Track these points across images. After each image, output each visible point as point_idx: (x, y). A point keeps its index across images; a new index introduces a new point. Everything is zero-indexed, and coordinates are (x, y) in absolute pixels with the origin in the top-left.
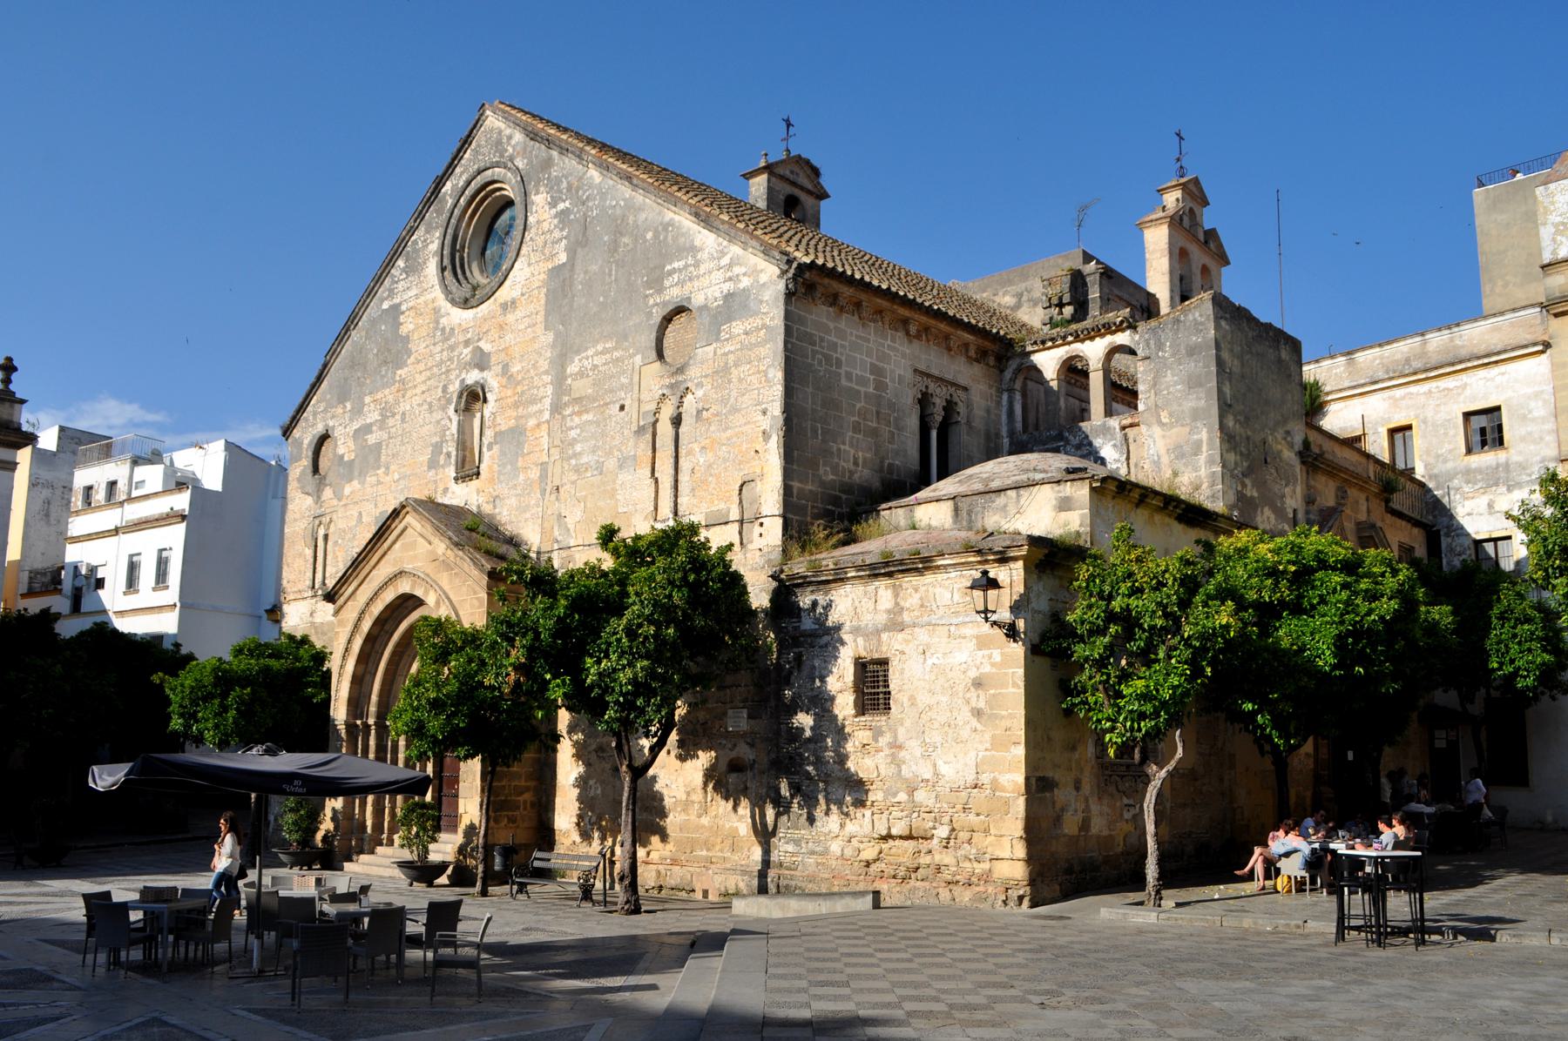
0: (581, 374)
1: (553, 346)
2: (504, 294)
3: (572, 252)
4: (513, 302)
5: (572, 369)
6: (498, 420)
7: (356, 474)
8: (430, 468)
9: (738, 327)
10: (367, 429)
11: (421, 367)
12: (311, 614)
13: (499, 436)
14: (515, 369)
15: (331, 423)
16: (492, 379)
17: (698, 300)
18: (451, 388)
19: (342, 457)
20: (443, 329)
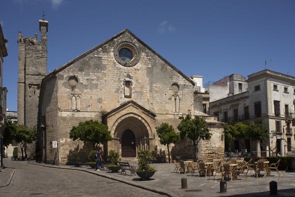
0: (156, 87)
1: (149, 80)
2: (135, 67)
3: (153, 66)
4: (138, 70)
5: (154, 85)
6: (136, 88)
7: (89, 88)
8: (115, 93)
9: (186, 89)
10: (93, 80)
11: (111, 72)
12: (73, 115)
13: (136, 92)
14: (140, 81)
15: (77, 75)
16: (133, 81)
17: (179, 83)
18: (121, 79)
19: (82, 83)
20: (117, 68)
